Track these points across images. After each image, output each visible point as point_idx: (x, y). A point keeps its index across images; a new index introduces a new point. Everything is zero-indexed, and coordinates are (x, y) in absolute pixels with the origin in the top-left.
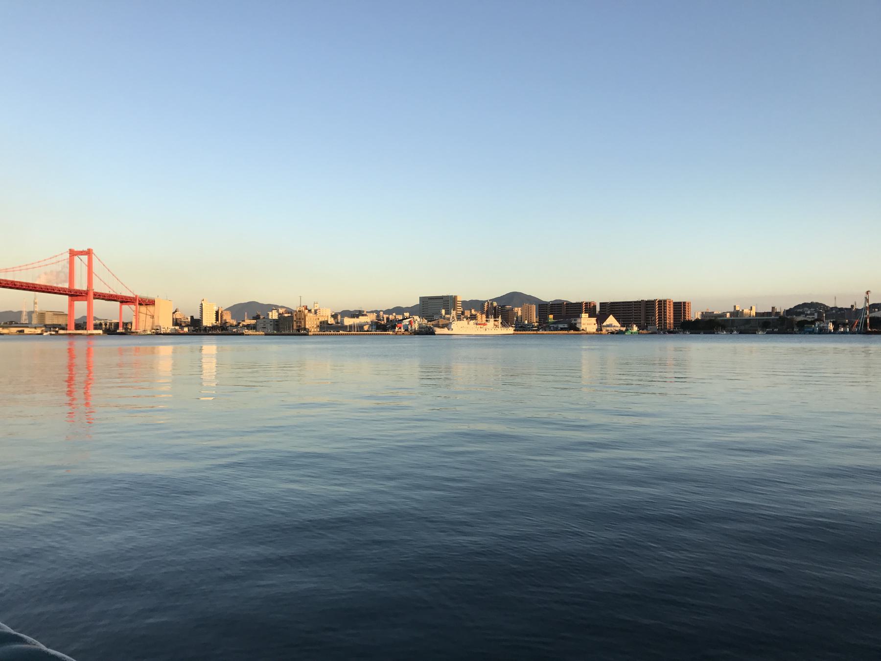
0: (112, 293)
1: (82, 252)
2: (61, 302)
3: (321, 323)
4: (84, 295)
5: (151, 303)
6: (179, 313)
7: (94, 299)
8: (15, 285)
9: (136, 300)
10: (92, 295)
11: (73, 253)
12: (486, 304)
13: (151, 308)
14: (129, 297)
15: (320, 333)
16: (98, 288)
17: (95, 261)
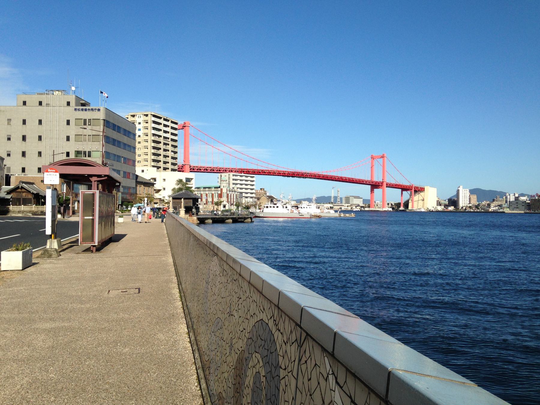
0: (397, 183)
4: (380, 184)
7: (387, 187)
8: (343, 179)
9: (412, 187)
13: (422, 194)
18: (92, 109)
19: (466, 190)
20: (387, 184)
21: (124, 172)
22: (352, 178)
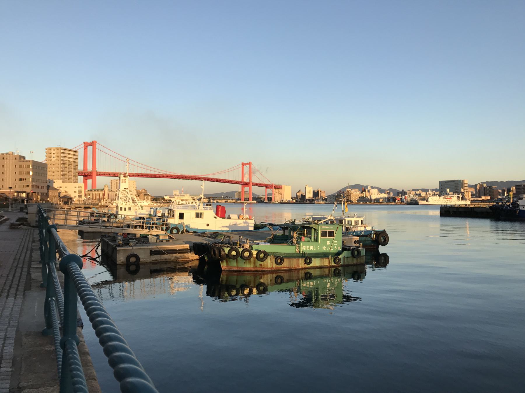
0: (262, 183)
1: (247, 164)
2: (238, 187)
3: (359, 197)
5: (280, 187)
6: (301, 192)
7: (252, 186)
8: (218, 180)
9: (273, 186)
10: (251, 185)
11: (243, 164)
12: (478, 185)
13: (280, 190)
14: (269, 185)
15: (358, 203)
16: (254, 180)
17: (252, 167)
18: (27, 161)
19: (310, 187)
20: (252, 184)
21: (41, 186)
22: (225, 180)
